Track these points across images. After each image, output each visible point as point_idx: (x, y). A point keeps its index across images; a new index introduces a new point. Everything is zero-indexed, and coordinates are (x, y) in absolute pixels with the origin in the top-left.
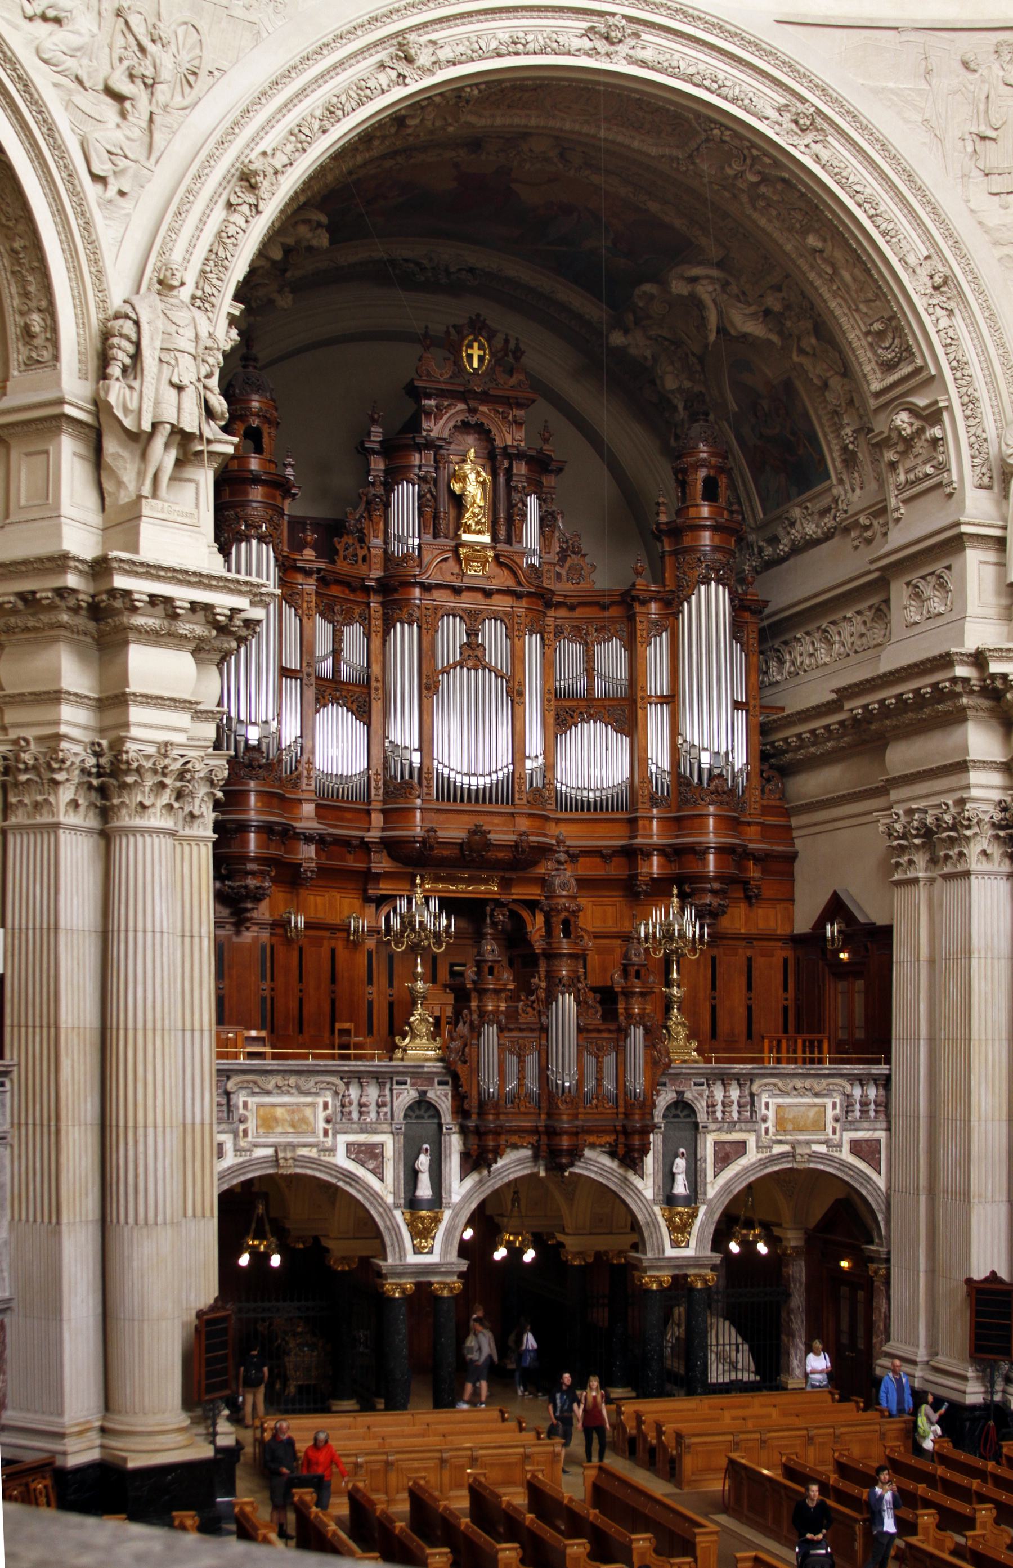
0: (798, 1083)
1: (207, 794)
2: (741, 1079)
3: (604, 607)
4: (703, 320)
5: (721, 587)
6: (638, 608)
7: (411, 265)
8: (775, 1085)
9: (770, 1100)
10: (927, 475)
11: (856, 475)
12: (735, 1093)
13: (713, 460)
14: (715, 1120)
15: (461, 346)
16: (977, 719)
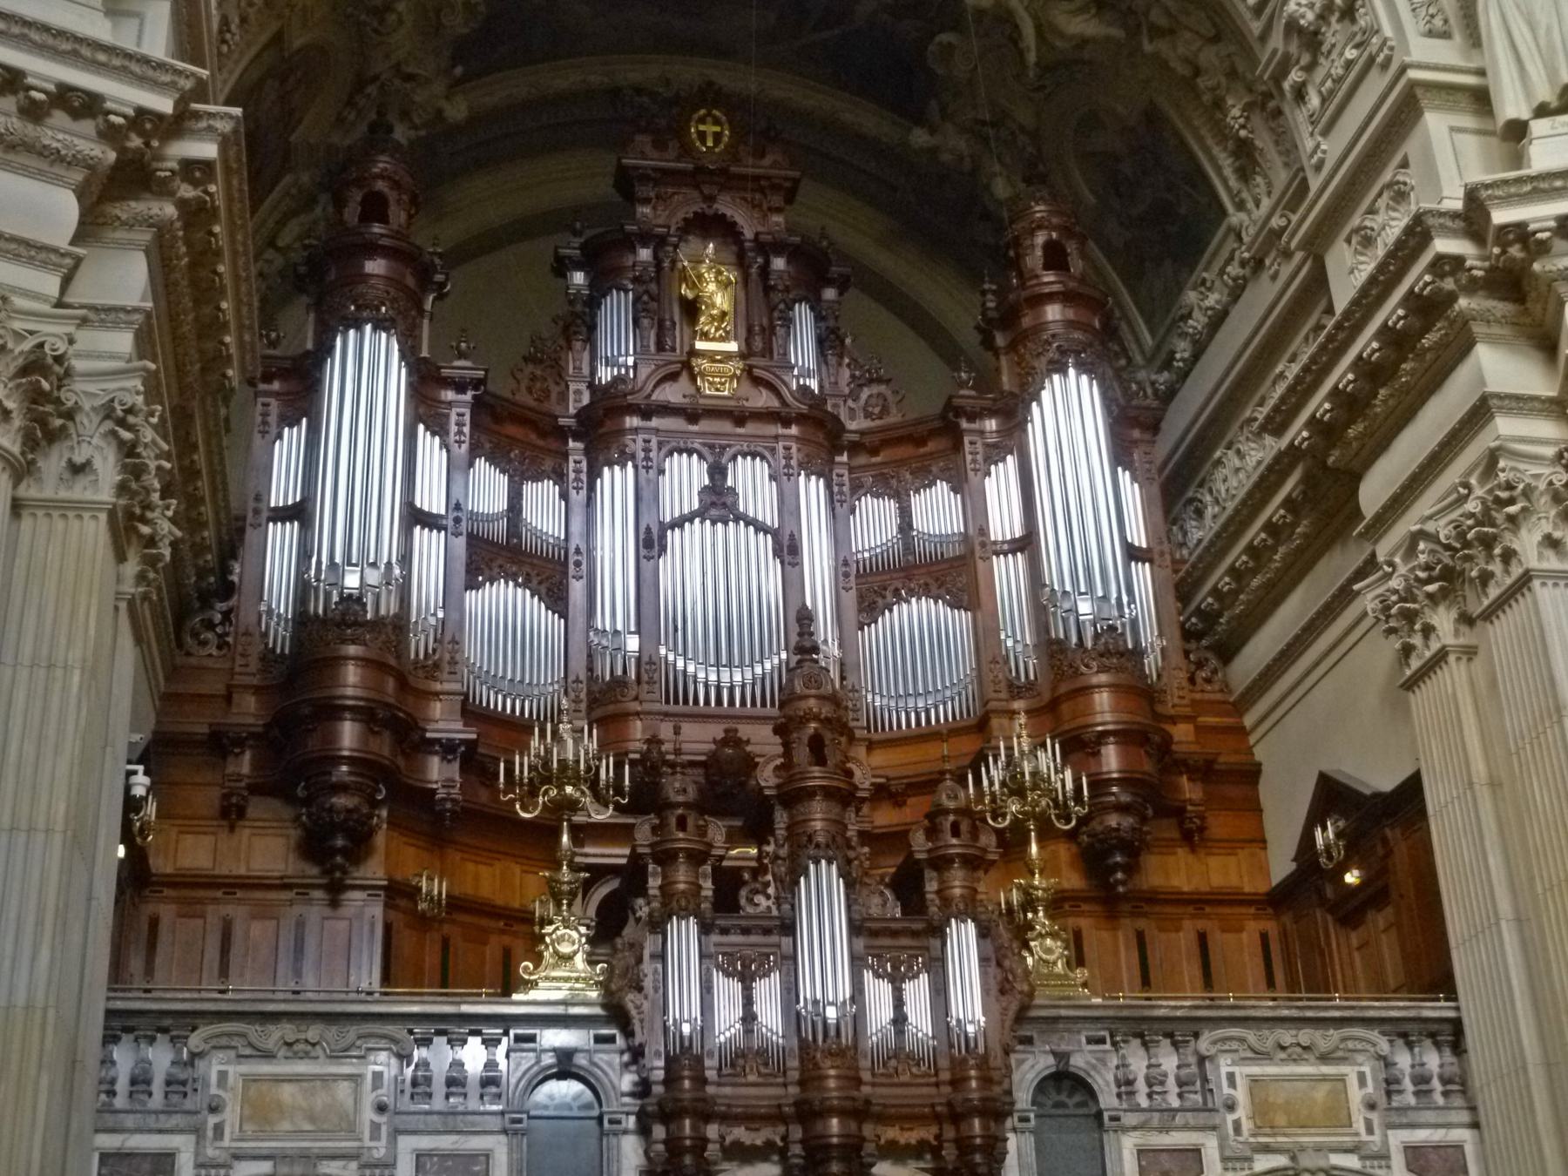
0: (1287, 1036)
1: (105, 435)
2: (1179, 1031)
3: (920, 441)
4: (1015, 38)
5: (1084, 378)
6: (964, 424)
7: (645, 99)
8: (1242, 1040)
9: (1236, 1070)
10: (1349, 64)
11: (1259, 179)
12: (1169, 1062)
13: (1055, 220)
14: (1137, 1109)
15: (689, 120)
16: (1492, 340)
